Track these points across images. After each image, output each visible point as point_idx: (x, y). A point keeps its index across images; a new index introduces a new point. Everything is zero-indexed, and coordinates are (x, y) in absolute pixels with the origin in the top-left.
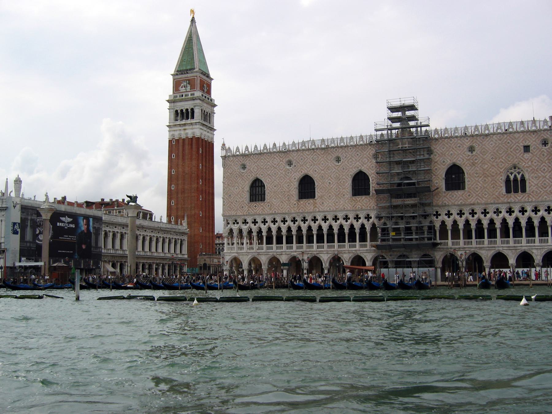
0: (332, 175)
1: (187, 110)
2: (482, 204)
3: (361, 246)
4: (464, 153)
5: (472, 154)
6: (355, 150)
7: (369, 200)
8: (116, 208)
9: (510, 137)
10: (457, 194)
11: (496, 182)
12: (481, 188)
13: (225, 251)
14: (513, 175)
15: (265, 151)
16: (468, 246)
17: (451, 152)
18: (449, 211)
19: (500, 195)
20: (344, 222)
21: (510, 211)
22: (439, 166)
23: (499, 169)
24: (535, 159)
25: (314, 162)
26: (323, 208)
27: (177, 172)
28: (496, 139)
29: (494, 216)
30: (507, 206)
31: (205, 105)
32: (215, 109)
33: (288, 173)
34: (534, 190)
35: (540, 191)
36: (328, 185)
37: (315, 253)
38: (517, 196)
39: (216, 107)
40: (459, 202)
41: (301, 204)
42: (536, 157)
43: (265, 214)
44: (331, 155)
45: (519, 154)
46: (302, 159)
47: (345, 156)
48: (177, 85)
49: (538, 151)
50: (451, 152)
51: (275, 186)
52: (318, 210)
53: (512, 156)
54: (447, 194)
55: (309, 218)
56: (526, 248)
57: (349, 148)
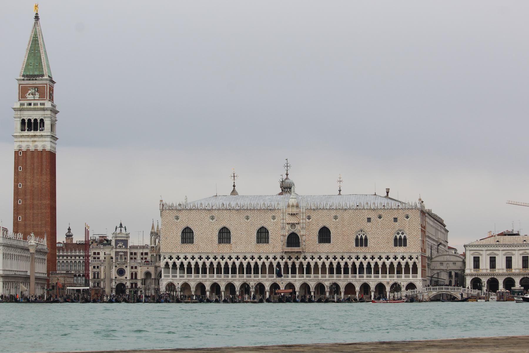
0: (243, 229)
1: (36, 120)
2: (340, 253)
3: (262, 277)
5: (336, 221)
7: (269, 247)
9: (360, 212)
10: (325, 245)
11: (350, 239)
13: (162, 278)
14: (360, 235)
15: (194, 208)
16: (331, 279)
17: (323, 219)
18: (320, 256)
20: (250, 260)
23: (352, 231)
24: (373, 227)
25: (231, 218)
27: (25, 186)
28: (351, 212)
29: (348, 260)
30: (356, 254)
32: (57, 115)
33: (211, 225)
35: (375, 246)
36: (240, 235)
37: (231, 280)
38: (362, 249)
40: (327, 250)
42: (375, 225)
43: (193, 253)
44: (243, 215)
45: (364, 223)
46: (222, 216)
47: (253, 216)
48: (23, 92)
49: (375, 221)
50: (323, 219)
53: (360, 224)
55: (226, 257)
56: (366, 281)
57: (256, 211)
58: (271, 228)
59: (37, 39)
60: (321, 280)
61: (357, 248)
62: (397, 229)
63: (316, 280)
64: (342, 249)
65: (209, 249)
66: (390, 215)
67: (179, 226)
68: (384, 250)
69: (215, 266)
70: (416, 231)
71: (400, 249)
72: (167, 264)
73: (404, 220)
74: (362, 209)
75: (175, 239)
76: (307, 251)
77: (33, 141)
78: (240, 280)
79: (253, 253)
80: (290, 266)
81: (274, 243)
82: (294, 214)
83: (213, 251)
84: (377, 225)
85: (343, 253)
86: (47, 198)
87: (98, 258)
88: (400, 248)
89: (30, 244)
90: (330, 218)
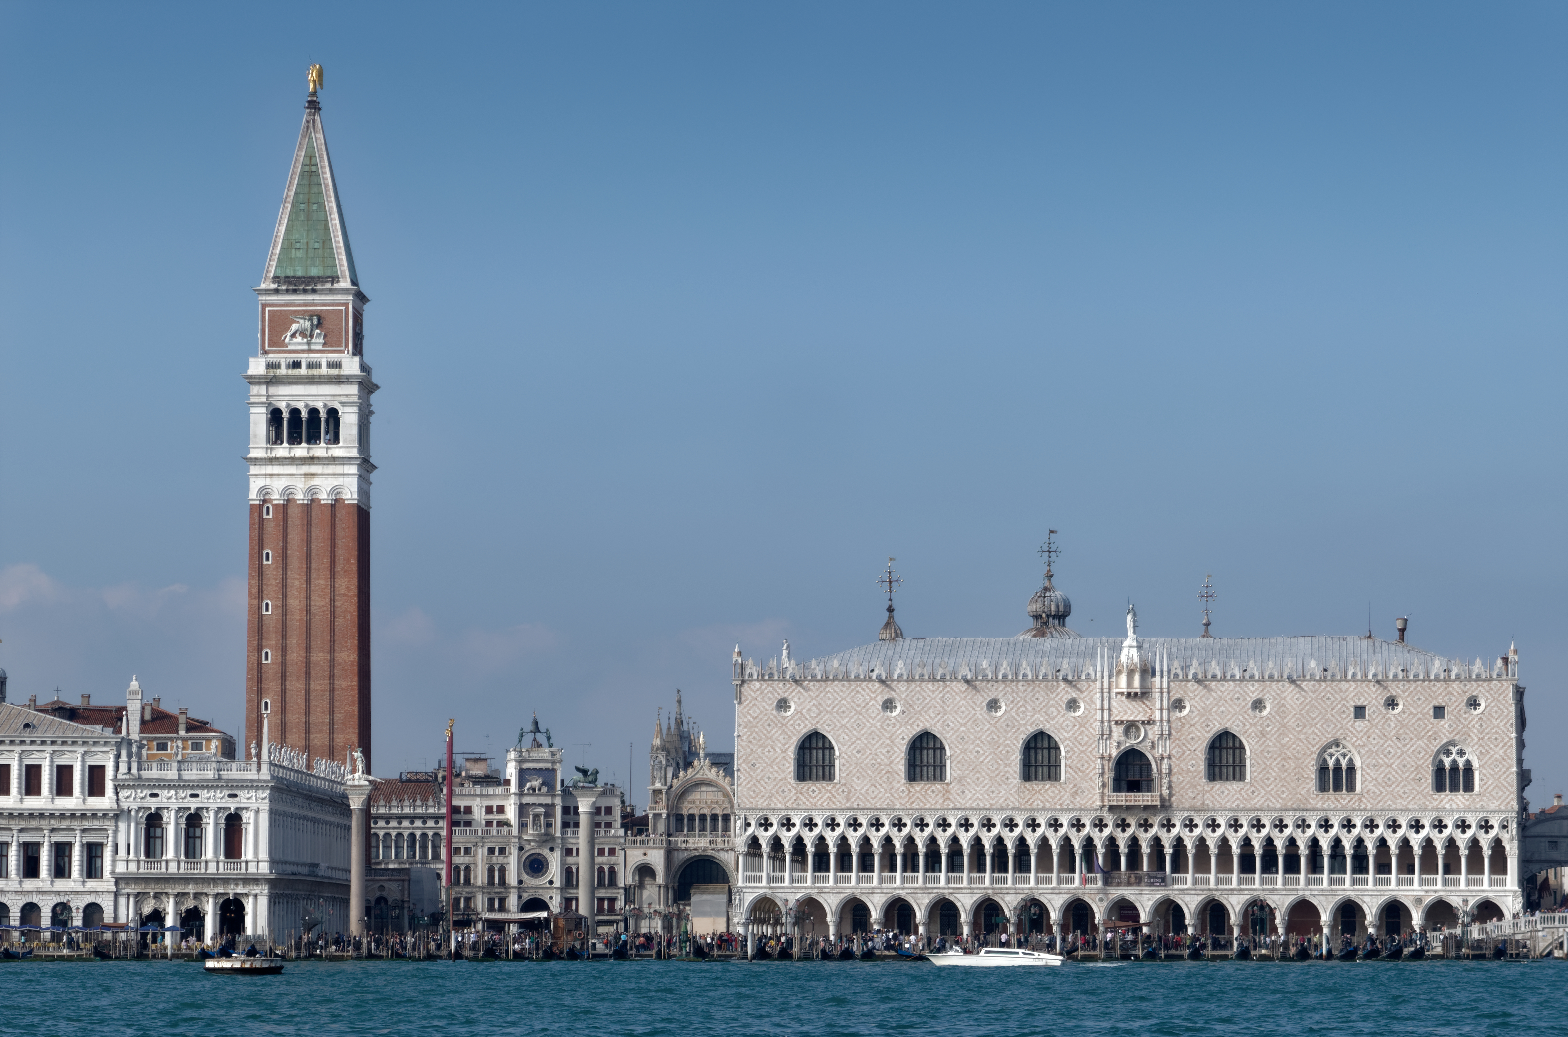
1: (314, 412)
2: (1276, 810)
4: (1245, 712)
6: (1033, 689)
8: (182, 733)
9: (1332, 688)
10: (1230, 788)
14: (1334, 758)
21: (1326, 825)
22: (1198, 734)
23: (1310, 746)
25: (945, 707)
32: (374, 398)
33: (888, 725)
36: (975, 757)
39: (377, 393)
40: (1233, 803)
41: (917, 792)
42: (1377, 728)
43: (836, 809)
46: (918, 699)
47: (1011, 699)
49: (1380, 717)
50: (1223, 708)
51: (858, 752)
52: (952, 806)
53: (1334, 723)
54: (1212, 788)
57: (1021, 683)
58: (1067, 736)
59: (314, 169)
60: (1216, 890)
61: (1326, 797)
62: (1446, 740)
63: (1203, 890)
64: (1282, 798)
65: (880, 798)
66: (1423, 699)
67: (791, 728)
69: (899, 849)
70: (1502, 744)
72: (754, 842)
73: (1465, 713)
74: (1340, 681)
75: (779, 768)
77: (305, 474)
78: (975, 891)
79: (1012, 809)
80: (1123, 849)
81: (1075, 779)
82: (1136, 694)
83: (895, 805)
85: (1282, 810)
86: (349, 644)
87: (468, 824)
88: (1454, 798)
89: (350, 783)
90: (1244, 707)
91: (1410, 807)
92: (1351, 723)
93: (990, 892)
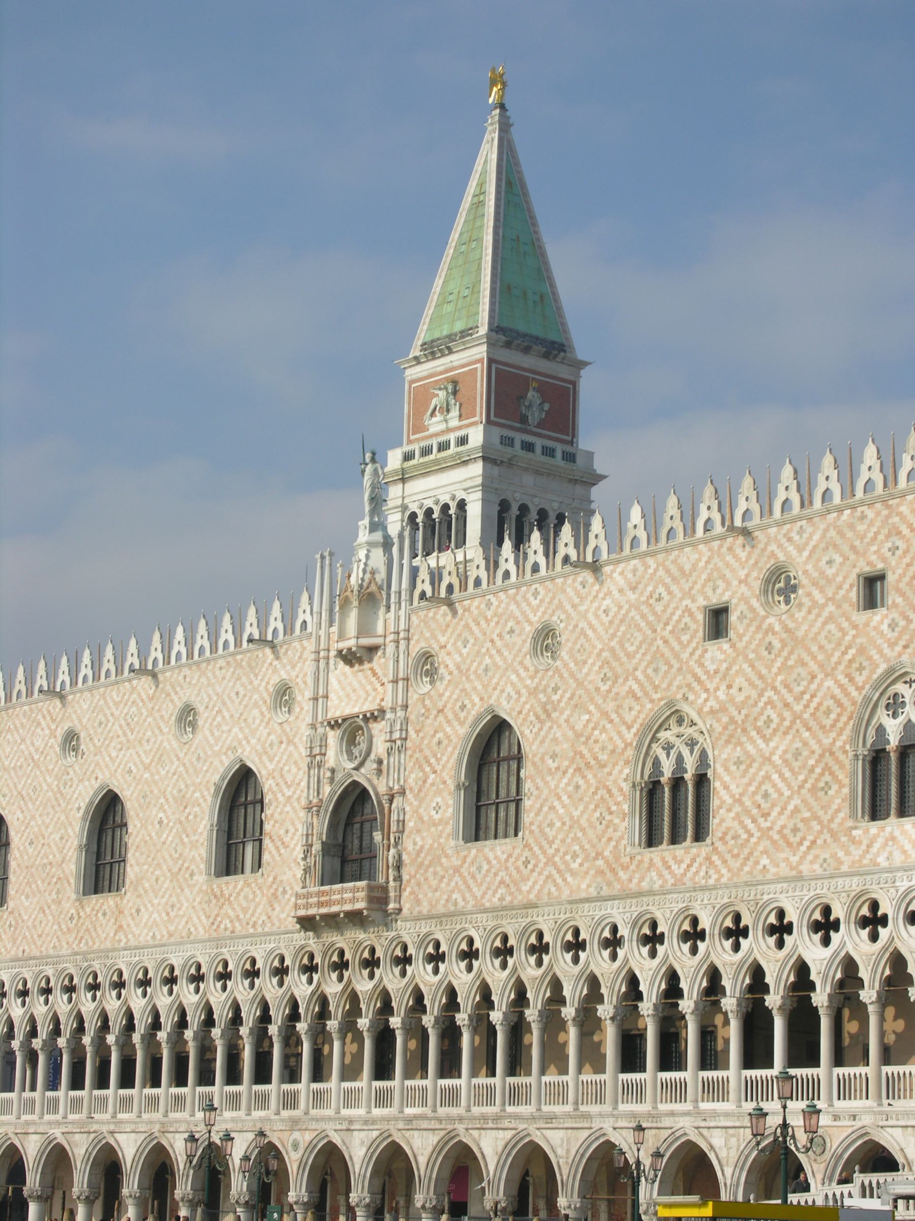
1: (446, 507)
6: (234, 673)
9: (668, 571)
10: (491, 855)
12: (564, 824)
17: (487, 660)
19: (617, 858)
22: (448, 729)
23: (623, 729)
26: (137, 932)
31: (529, 480)
32: (596, 492)
34: (728, 829)
36: (157, 833)
40: (495, 892)
44: (172, 701)
45: (690, 650)
49: (752, 629)
50: (487, 660)
51: (31, 843)
58: (271, 767)
62: (882, 667)
65: (48, 935)
68: (794, 860)
71: (893, 838)
76: (405, 911)
84: (759, 657)
88: (897, 833)
91: (805, 868)
92: (699, 652)
93: (156, 1128)
